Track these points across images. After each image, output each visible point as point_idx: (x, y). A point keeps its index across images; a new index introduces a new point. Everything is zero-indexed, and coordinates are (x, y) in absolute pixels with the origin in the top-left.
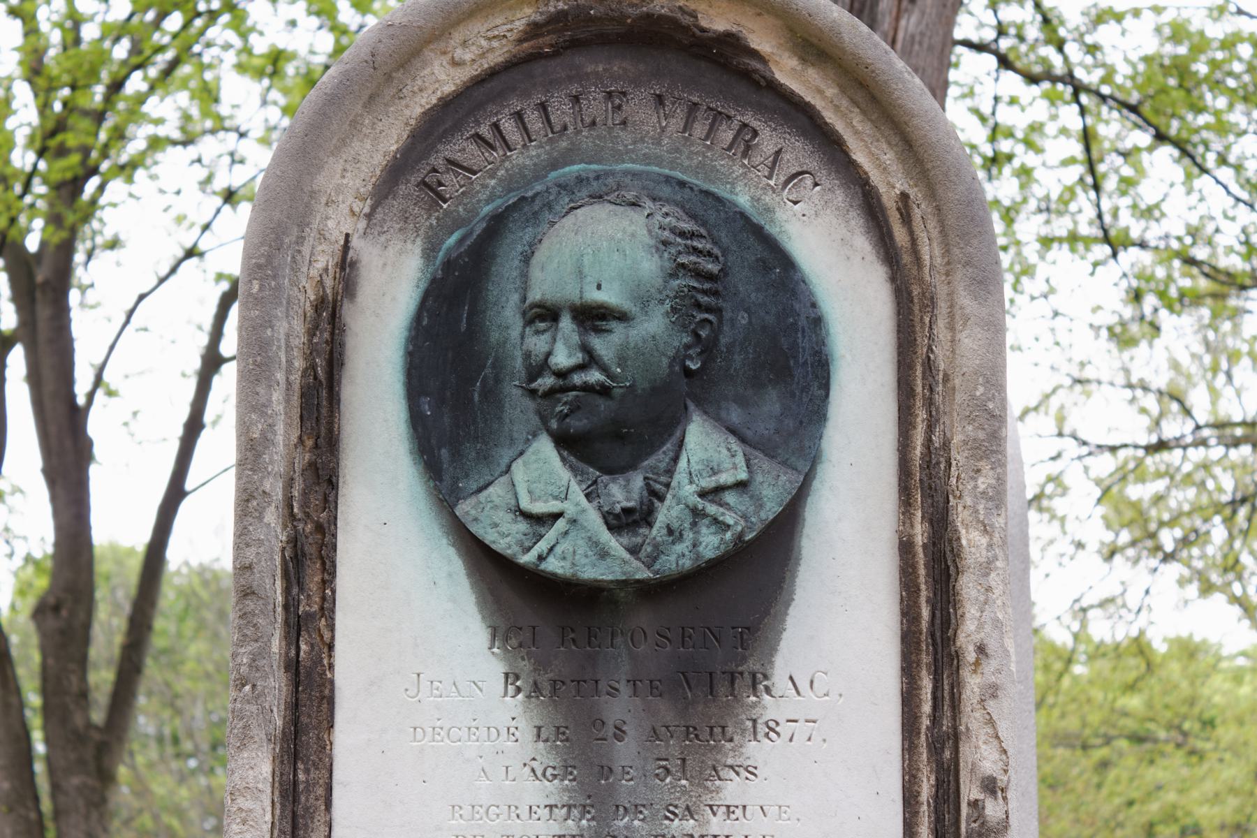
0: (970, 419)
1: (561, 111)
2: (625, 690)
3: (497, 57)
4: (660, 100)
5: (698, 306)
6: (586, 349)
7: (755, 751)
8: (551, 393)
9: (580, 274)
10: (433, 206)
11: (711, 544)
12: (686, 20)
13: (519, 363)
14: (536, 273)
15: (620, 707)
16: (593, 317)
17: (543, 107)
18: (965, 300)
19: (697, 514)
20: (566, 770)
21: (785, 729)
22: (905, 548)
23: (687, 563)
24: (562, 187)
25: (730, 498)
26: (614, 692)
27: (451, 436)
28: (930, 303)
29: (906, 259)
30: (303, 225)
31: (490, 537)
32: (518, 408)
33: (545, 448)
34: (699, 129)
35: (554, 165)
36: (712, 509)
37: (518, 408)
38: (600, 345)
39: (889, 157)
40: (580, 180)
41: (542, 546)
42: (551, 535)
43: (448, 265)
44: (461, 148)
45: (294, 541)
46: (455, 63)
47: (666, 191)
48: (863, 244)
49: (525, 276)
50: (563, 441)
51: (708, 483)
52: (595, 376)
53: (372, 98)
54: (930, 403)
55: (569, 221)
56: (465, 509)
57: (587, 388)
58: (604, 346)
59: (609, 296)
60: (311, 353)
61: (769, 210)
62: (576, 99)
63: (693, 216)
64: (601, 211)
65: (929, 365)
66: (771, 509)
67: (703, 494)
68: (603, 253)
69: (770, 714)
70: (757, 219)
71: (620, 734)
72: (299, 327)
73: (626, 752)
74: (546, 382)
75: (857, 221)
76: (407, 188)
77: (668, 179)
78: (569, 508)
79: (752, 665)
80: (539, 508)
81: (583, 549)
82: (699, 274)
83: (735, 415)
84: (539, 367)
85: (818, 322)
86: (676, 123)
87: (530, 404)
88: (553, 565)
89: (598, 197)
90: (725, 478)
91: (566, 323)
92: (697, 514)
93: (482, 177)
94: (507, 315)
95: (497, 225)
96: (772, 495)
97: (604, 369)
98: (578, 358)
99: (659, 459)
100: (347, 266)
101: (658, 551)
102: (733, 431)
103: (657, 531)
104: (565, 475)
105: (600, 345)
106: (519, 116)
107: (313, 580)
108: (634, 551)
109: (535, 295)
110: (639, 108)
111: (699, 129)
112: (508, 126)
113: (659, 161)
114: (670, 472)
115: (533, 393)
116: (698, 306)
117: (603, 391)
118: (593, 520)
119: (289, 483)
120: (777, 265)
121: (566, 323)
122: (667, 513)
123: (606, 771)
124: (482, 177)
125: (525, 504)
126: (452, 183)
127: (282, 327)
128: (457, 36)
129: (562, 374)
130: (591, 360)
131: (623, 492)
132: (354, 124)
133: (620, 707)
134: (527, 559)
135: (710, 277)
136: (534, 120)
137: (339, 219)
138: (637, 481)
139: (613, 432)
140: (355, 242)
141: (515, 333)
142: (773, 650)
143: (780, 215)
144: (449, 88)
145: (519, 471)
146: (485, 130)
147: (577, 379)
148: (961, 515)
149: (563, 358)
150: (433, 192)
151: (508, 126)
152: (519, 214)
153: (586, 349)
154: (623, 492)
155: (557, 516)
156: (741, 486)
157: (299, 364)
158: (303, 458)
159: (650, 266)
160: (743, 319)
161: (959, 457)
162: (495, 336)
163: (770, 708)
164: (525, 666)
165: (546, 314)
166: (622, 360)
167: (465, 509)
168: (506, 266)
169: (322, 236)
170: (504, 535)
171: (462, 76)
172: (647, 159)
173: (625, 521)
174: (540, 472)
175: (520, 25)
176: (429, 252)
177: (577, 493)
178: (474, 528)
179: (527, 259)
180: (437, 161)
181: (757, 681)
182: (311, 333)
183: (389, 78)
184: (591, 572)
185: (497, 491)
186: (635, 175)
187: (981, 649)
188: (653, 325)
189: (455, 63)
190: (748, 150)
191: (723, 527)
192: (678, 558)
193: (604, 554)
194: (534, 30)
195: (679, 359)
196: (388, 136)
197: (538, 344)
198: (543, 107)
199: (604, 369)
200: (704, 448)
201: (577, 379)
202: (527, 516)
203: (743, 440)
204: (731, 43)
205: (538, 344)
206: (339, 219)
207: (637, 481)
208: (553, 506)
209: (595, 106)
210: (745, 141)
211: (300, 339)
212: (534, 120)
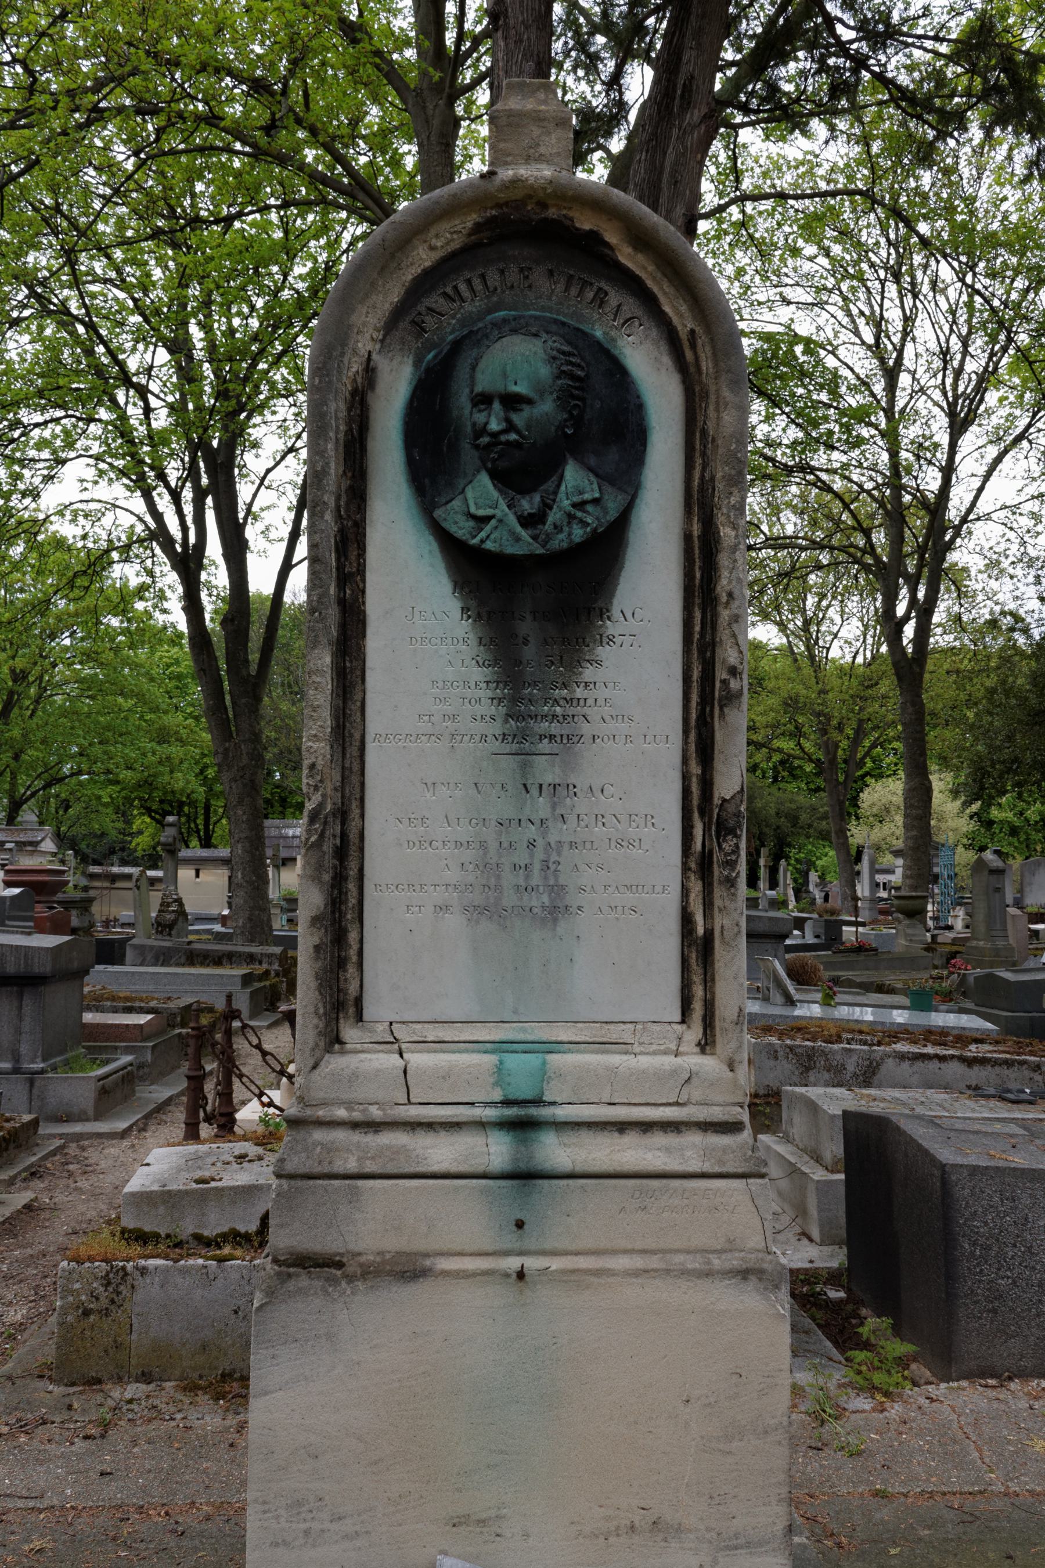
0: (727, 463)
1: (494, 279)
2: (529, 617)
3: (455, 245)
4: (551, 273)
5: (574, 397)
6: (508, 420)
7: (603, 652)
8: (489, 445)
9: (505, 375)
10: (419, 336)
11: (578, 534)
12: (568, 223)
13: (469, 429)
14: (479, 376)
15: (526, 627)
16: (512, 402)
17: (483, 277)
18: (726, 393)
19: (571, 517)
20: (495, 663)
21: (618, 640)
22: (687, 538)
23: (565, 545)
24: (494, 324)
25: (590, 508)
26: (523, 619)
27: (431, 474)
28: (705, 395)
29: (692, 369)
30: (344, 345)
31: (453, 529)
32: (469, 456)
33: (484, 479)
34: (574, 291)
35: (490, 311)
36: (579, 514)
37: (469, 456)
38: (515, 418)
39: (684, 308)
40: (505, 321)
41: (483, 534)
42: (488, 528)
43: (428, 370)
44: (435, 301)
45: (342, 531)
46: (432, 248)
47: (554, 328)
48: (667, 360)
49: (472, 378)
50: (495, 476)
51: (576, 499)
52: (513, 437)
53: (383, 269)
54: (703, 454)
55: (498, 345)
56: (438, 513)
57: (508, 443)
58: (518, 419)
59: (520, 389)
60: (349, 422)
61: (614, 340)
62: (502, 272)
63: (569, 343)
64: (517, 339)
65: (704, 432)
66: (613, 515)
67: (574, 505)
68: (518, 362)
69: (610, 631)
70: (607, 345)
71: (526, 642)
72: (342, 406)
73: (529, 652)
74: (485, 440)
75: (664, 347)
76: (404, 324)
77: (556, 321)
78: (498, 513)
79: (600, 604)
80: (481, 513)
81: (506, 537)
82: (572, 377)
83: (592, 461)
84: (481, 431)
85: (640, 407)
86: (560, 287)
87: (476, 453)
88: (489, 545)
89: (514, 331)
90: (587, 496)
91: (497, 406)
92: (571, 517)
93: (447, 317)
94: (462, 400)
95: (457, 347)
96: (613, 506)
97: (518, 432)
98: (503, 425)
99: (550, 485)
100: (370, 371)
101: (549, 537)
102: (591, 469)
103: (548, 527)
104: (495, 494)
105: (515, 418)
106: (469, 282)
107: (353, 555)
108: (535, 538)
109: (478, 389)
110: (539, 278)
111: (574, 291)
112: (463, 287)
113: (550, 310)
114: (556, 493)
115: (477, 447)
116: (574, 397)
117: (516, 445)
118: (512, 519)
119: (338, 498)
120: (618, 373)
121: (497, 406)
122: (554, 516)
123: (518, 662)
124: (447, 317)
125: (473, 510)
126: (430, 322)
127: (333, 406)
128: (433, 231)
129: (494, 435)
130: (511, 427)
131: (528, 505)
132: (373, 284)
133: (526, 627)
134: (475, 541)
135: (578, 379)
136: (477, 283)
137: (364, 344)
138: (537, 498)
139: (523, 470)
140: (374, 356)
141: (467, 412)
142: (612, 595)
143: (620, 343)
144: (428, 264)
145: (470, 493)
146: (449, 290)
147: (503, 438)
148: (720, 519)
149: (494, 426)
150: (419, 327)
151: (463, 287)
152: (470, 340)
153: (508, 420)
154: (528, 505)
155: (489, 518)
156: (595, 501)
157: (343, 428)
158: (346, 483)
159: (545, 372)
160: (598, 405)
161: (720, 486)
162: (455, 413)
163: (611, 628)
164: (473, 603)
165: (483, 400)
166: (528, 427)
167: (438, 513)
168: (462, 372)
169: (355, 352)
170: (460, 528)
171: (436, 256)
172: (543, 309)
173: (529, 521)
174: (481, 492)
175: (469, 225)
176: (417, 364)
177: (503, 506)
178: (444, 525)
179: (473, 368)
180: (421, 308)
181: (604, 613)
182: (349, 410)
183: (392, 256)
184: (511, 549)
185: (456, 503)
186: (536, 318)
187: (730, 595)
188: (546, 407)
189: (432, 248)
190: (602, 304)
191: (586, 524)
192: (560, 542)
193: (518, 539)
194: (478, 228)
195: (561, 427)
196: (392, 294)
197: (480, 418)
198: (483, 277)
199: (518, 432)
200: (574, 479)
201: (503, 438)
202: (474, 517)
203: (597, 475)
204: (594, 237)
205: (480, 418)
206: (364, 344)
207: (537, 498)
208: (489, 512)
209: (513, 275)
210: (600, 299)
211: (343, 414)
212: (477, 283)
